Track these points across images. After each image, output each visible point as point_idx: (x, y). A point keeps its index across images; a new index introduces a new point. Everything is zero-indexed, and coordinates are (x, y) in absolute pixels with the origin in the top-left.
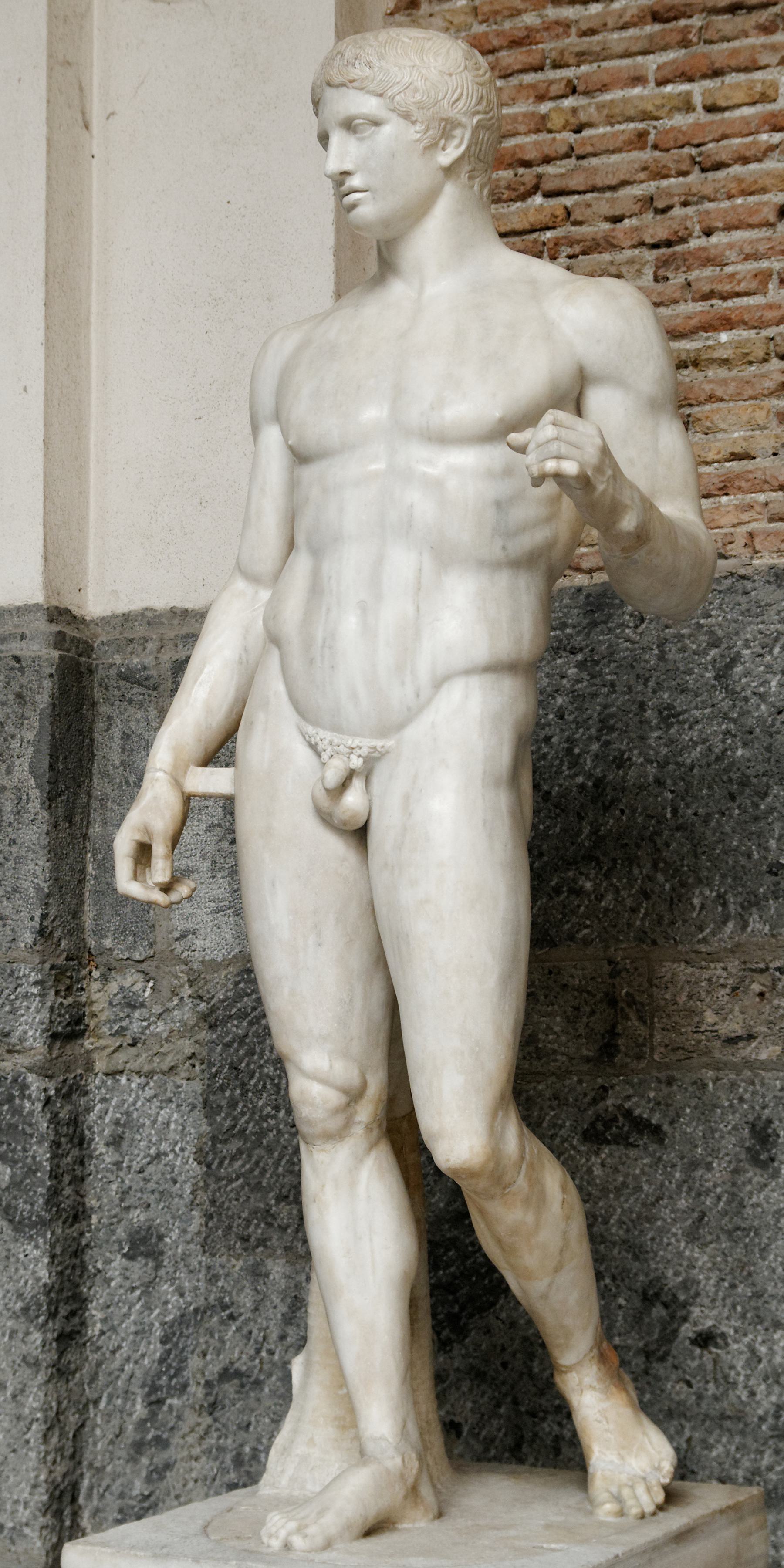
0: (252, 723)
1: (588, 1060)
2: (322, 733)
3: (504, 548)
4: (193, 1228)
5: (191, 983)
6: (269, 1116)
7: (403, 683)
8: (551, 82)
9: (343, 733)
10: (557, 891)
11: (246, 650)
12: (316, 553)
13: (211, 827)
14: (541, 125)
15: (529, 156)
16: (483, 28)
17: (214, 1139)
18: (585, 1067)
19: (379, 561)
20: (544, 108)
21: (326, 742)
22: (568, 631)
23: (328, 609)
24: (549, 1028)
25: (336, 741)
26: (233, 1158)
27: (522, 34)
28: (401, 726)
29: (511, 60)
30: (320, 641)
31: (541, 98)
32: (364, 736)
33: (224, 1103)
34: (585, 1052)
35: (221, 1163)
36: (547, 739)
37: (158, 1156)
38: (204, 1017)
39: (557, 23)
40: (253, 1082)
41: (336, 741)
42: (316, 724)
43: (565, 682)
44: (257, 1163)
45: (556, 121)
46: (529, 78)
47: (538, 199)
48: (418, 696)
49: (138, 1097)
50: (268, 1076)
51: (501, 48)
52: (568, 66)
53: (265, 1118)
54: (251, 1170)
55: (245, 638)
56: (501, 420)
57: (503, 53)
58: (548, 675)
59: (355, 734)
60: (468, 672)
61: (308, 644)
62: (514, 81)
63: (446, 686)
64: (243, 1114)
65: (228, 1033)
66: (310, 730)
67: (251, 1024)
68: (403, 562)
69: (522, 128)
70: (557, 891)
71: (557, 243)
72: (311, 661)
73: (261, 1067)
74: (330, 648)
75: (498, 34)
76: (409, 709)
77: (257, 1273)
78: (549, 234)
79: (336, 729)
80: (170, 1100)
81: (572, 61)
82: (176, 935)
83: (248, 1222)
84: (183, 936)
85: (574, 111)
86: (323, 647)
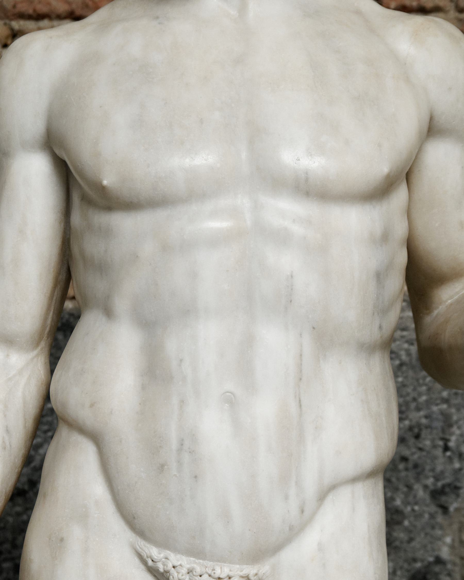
0: (62, 540)
2: (174, 559)
3: (380, 327)
7: (286, 498)
9: (204, 559)
11: (7, 431)
12: (151, 325)
19: (249, 342)
21: (184, 571)
23: (182, 402)
25: (198, 570)
28: (277, 548)
30: (174, 444)
32: (231, 562)
41: (198, 570)
42: (164, 544)
48: (302, 511)
55: (5, 416)
56: (388, 177)
59: (222, 560)
60: (354, 480)
61: (154, 446)
63: (330, 497)
66: (154, 552)
68: (277, 344)
72: (162, 467)
74: (191, 452)
76: (291, 528)
79: (196, 552)
86: (180, 450)
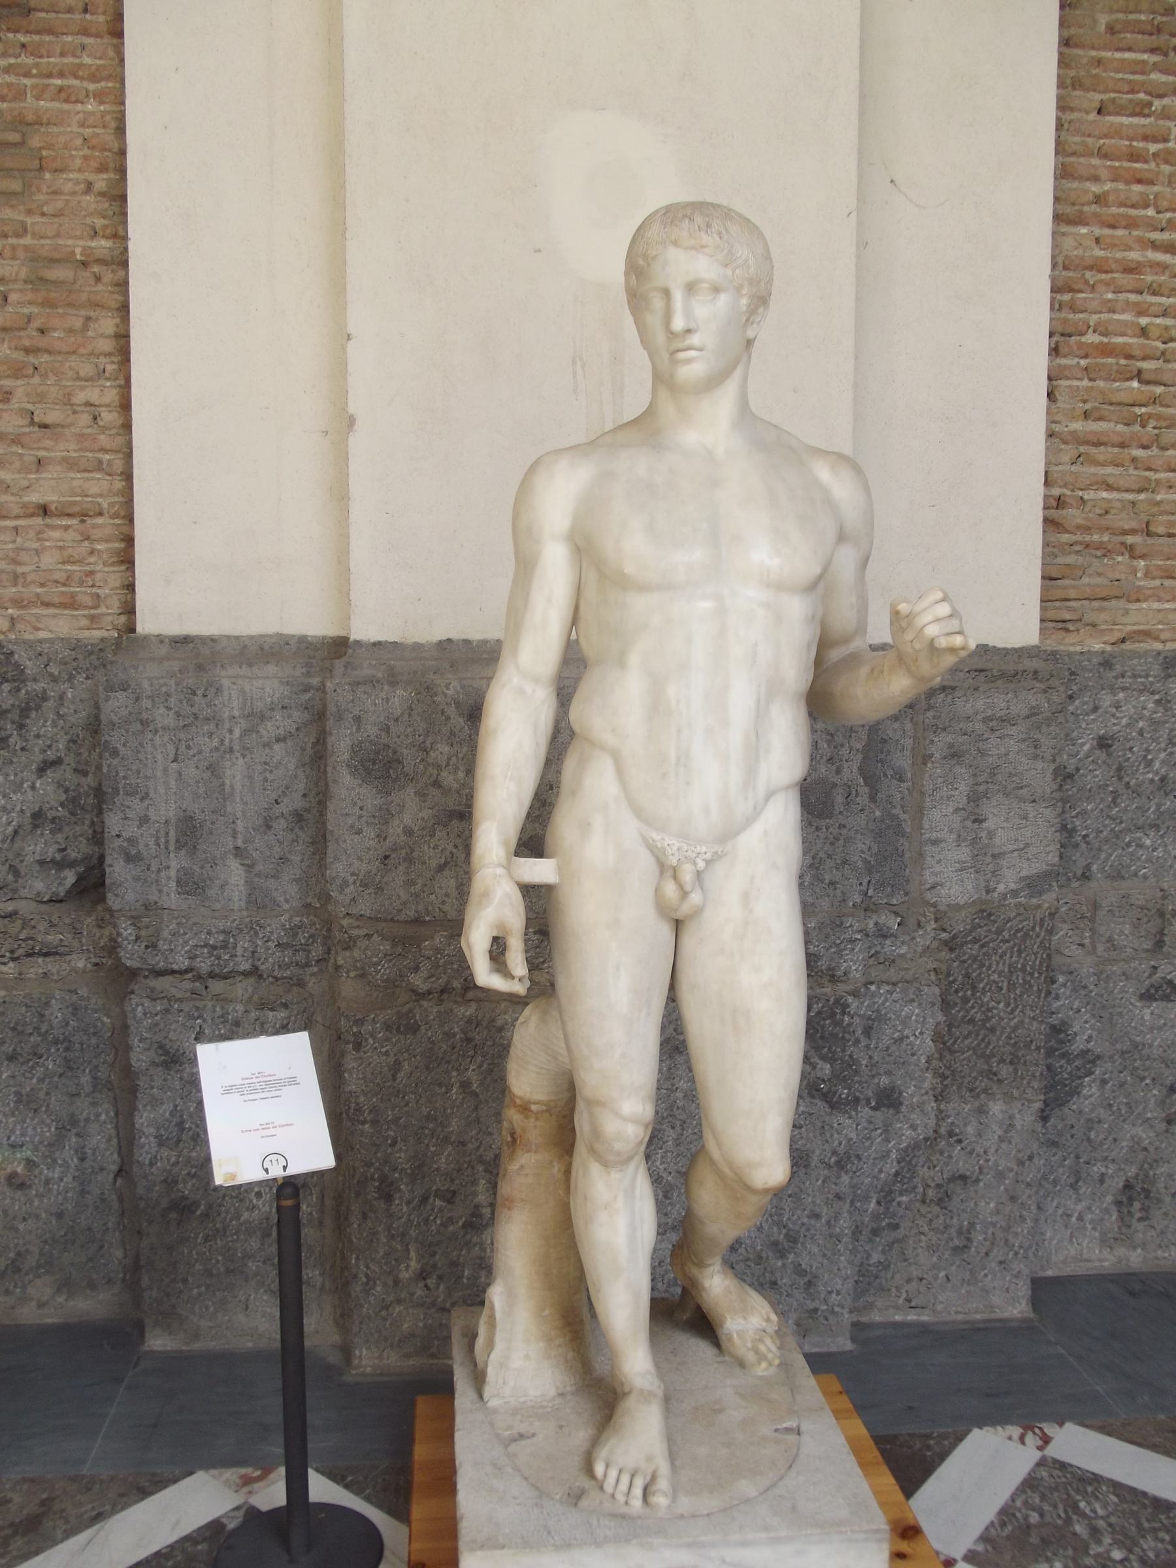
1: (1147, 951)
4: (927, 1085)
5: (936, 920)
6: (993, 1008)
8: (1151, 304)
10: (1128, 845)
13: (957, 810)
14: (1144, 332)
15: (1137, 352)
16: (1101, 253)
17: (950, 1026)
18: (1144, 955)
20: (1144, 321)
22: (1151, 679)
24: (1121, 931)
26: (966, 1037)
27: (1133, 265)
29: (1125, 282)
31: (1140, 314)
33: (958, 1001)
34: (1145, 946)
35: (955, 1042)
36: (1131, 749)
37: (901, 1039)
38: (946, 943)
39: (1158, 264)
40: (981, 986)
43: (1145, 712)
44: (983, 1040)
45: (1155, 333)
46: (1133, 297)
47: (1135, 384)
49: (886, 1000)
50: (994, 981)
51: (1117, 272)
52: (1162, 295)
53: (989, 1010)
54: (979, 1045)
57: (1116, 275)
58: (1135, 707)
62: (1122, 296)
64: (973, 1007)
65: (964, 954)
67: (982, 946)
69: (1130, 332)
70: (1128, 845)
71: (1150, 416)
73: (989, 976)
75: (1116, 261)
77: (981, 1111)
78: (1143, 410)
80: (913, 1001)
81: (1166, 293)
82: (928, 886)
83: (976, 1078)
84: (933, 887)
85: (1167, 328)
